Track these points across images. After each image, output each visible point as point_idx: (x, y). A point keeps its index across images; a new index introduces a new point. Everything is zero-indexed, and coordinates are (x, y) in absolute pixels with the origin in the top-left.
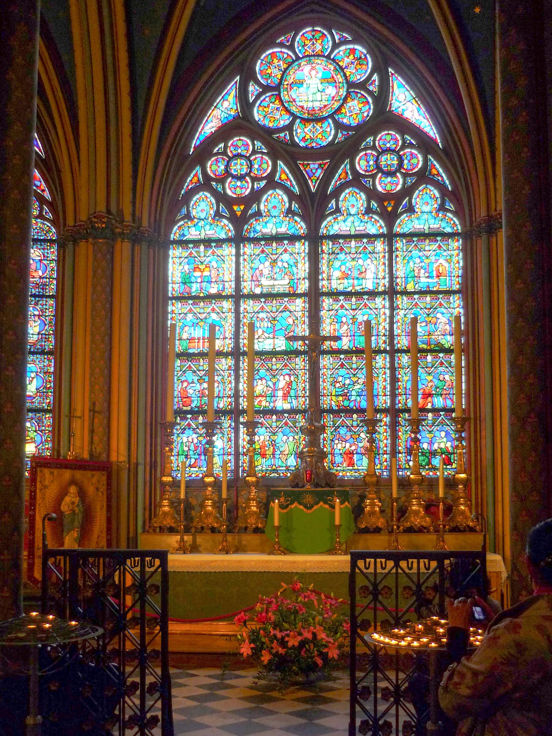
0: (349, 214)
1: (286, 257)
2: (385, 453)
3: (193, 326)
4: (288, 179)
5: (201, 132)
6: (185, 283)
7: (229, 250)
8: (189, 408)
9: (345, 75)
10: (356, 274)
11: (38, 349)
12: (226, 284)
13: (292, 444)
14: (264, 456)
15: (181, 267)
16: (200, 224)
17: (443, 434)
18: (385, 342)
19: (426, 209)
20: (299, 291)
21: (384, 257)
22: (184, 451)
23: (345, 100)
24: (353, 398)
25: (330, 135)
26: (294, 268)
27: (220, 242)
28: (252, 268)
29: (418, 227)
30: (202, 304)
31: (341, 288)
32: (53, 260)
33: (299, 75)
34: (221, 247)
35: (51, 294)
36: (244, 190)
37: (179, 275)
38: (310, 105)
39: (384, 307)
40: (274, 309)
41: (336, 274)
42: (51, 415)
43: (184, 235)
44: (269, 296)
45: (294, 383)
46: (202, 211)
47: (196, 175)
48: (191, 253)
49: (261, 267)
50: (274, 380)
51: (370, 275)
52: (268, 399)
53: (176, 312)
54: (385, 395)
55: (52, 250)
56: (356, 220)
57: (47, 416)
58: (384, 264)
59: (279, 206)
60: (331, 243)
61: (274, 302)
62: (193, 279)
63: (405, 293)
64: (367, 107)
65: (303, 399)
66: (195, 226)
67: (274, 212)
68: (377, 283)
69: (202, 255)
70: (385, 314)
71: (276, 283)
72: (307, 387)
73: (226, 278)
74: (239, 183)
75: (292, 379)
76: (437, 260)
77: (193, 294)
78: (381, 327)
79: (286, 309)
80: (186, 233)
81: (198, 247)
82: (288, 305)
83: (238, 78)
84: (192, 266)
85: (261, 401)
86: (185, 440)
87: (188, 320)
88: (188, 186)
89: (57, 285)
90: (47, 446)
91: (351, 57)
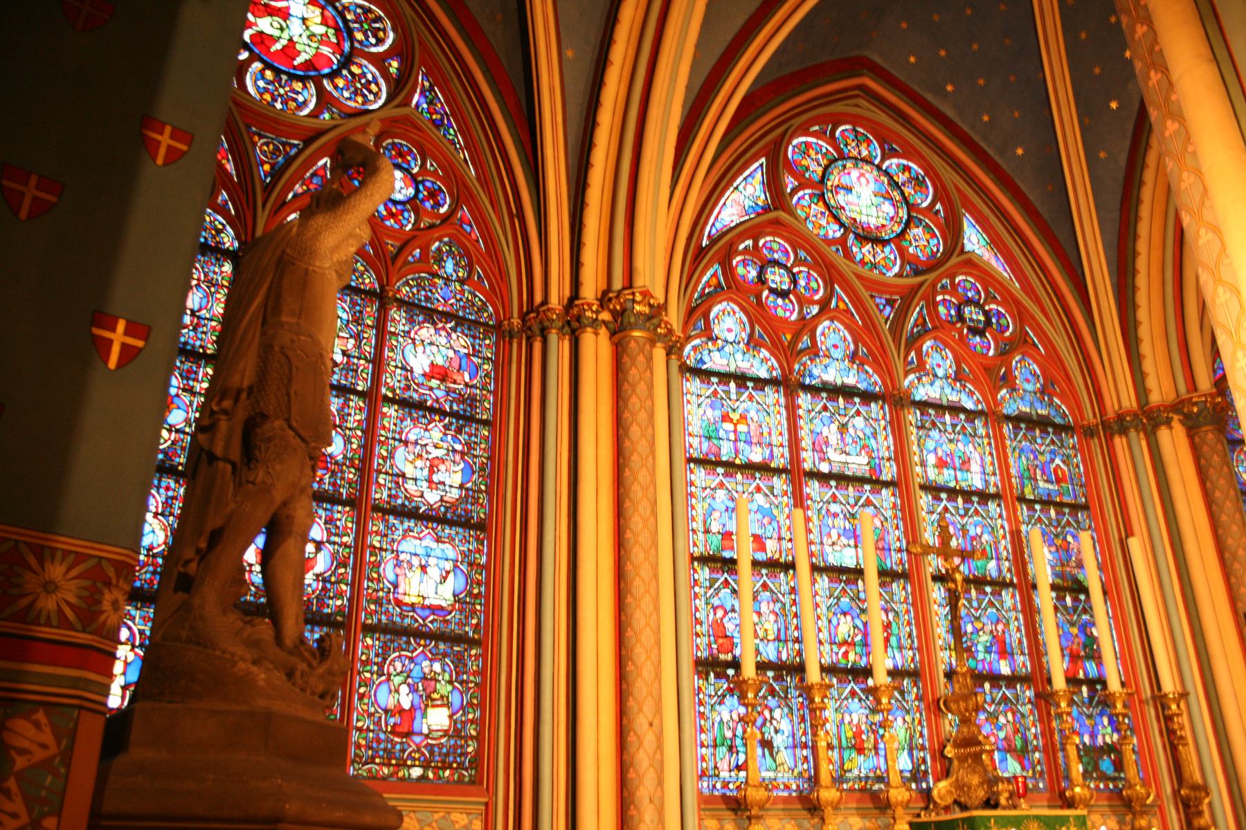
0: (935, 376)
1: (859, 422)
2: (1036, 749)
3: (727, 510)
4: (848, 311)
5: (717, 217)
6: (709, 438)
7: (772, 396)
8: (729, 657)
9: (902, 193)
10: (958, 463)
11: (460, 516)
12: (775, 449)
13: (903, 731)
14: (860, 750)
15: (701, 411)
16: (726, 349)
17: (1106, 721)
18: (1009, 570)
19: (1029, 387)
20: (883, 478)
21: (989, 444)
22: (725, 738)
23: (907, 225)
24: (981, 656)
25: (895, 264)
26: (872, 440)
27: (760, 383)
28: (812, 432)
29: (1024, 409)
30: (739, 476)
31: (941, 480)
32: (488, 359)
33: (845, 180)
34: (762, 390)
35: (485, 417)
36: (788, 314)
37: (699, 423)
38: (864, 219)
39: (1000, 516)
40: (852, 501)
41: (931, 459)
42: (480, 651)
43: (702, 361)
44: (843, 479)
45: (894, 625)
46: (730, 330)
47: (715, 275)
48: (715, 393)
49: (825, 432)
50: (864, 617)
51: (975, 467)
52: (858, 649)
53: (697, 483)
54: (1023, 653)
55: (487, 342)
56: (946, 386)
57: (473, 652)
58: (991, 454)
59: (840, 344)
60: (918, 412)
61: (851, 488)
62: (722, 434)
63: (1022, 499)
64: (935, 241)
65: (911, 653)
66: (719, 350)
67: (837, 354)
68: (986, 481)
69: (733, 397)
70: (1002, 527)
71: (849, 459)
72: (915, 633)
73: (776, 440)
74: (780, 301)
75: (891, 616)
76: (1052, 460)
77: (724, 459)
78: (1001, 548)
79: (868, 503)
80: (706, 358)
81: (727, 384)
82: (871, 497)
83: (763, 160)
84: (718, 413)
85: (846, 655)
86: (726, 717)
87: (718, 500)
88: (703, 289)
89: (495, 404)
90: (471, 716)
91: (907, 174)
